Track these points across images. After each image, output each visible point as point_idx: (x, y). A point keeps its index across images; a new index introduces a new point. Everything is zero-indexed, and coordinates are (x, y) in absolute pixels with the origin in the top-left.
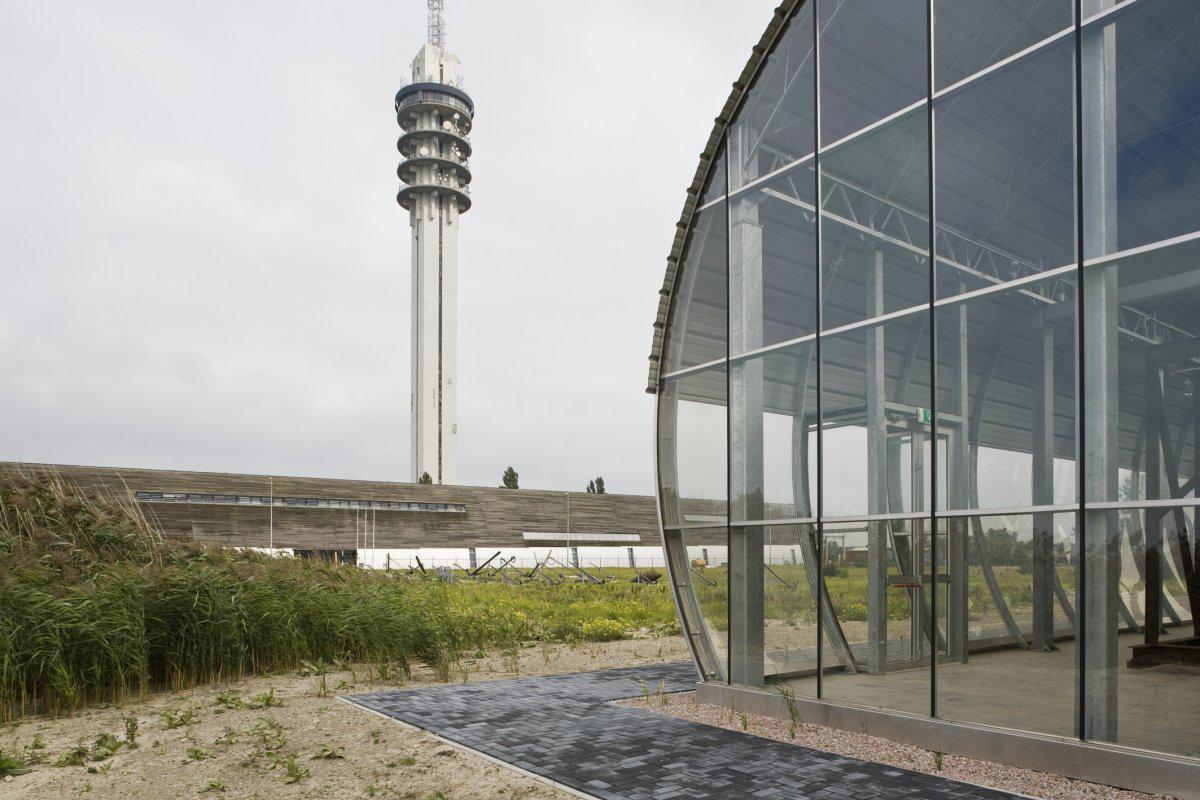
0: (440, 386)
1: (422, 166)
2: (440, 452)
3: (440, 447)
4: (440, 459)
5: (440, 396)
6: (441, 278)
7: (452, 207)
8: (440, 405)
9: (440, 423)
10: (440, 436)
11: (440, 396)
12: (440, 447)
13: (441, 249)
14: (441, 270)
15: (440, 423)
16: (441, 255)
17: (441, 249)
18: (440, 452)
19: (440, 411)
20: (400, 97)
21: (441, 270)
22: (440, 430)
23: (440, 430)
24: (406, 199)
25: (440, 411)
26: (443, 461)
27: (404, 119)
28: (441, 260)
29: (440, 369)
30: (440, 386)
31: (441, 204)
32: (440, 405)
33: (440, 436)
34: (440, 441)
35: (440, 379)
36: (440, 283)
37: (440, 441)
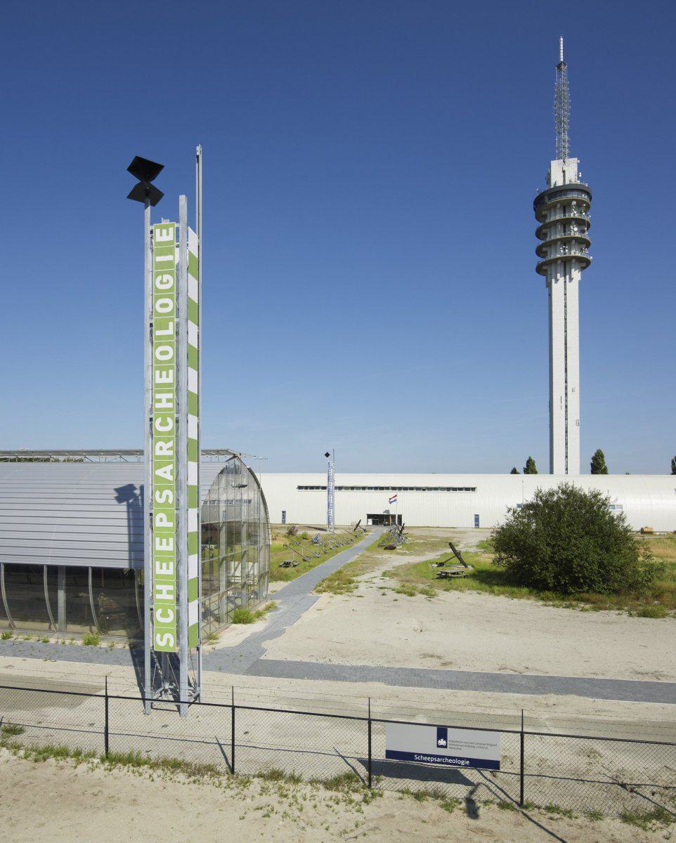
0: (566, 394)
1: (551, 246)
3: (566, 436)
5: (566, 401)
6: (566, 319)
7: (573, 270)
8: (566, 407)
9: (566, 419)
10: (566, 428)
11: (566, 401)
12: (566, 436)
13: (565, 299)
14: (566, 314)
16: (565, 303)
17: (565, 299)
19: (566, 411)
21: (566, 314)
22: (566, 425)
23: (566, 425)
24: (540, 269)
25: (566, 411)
27: (540, 217)
28: (565, 307)
29: (566, 382)
30: (566, 394)
31: (565, 268)
32: (566, 407)
33: (566, 428)
34: (566, 432)
35: (566, 389)
36: (566, 323)
37: (566, 432)
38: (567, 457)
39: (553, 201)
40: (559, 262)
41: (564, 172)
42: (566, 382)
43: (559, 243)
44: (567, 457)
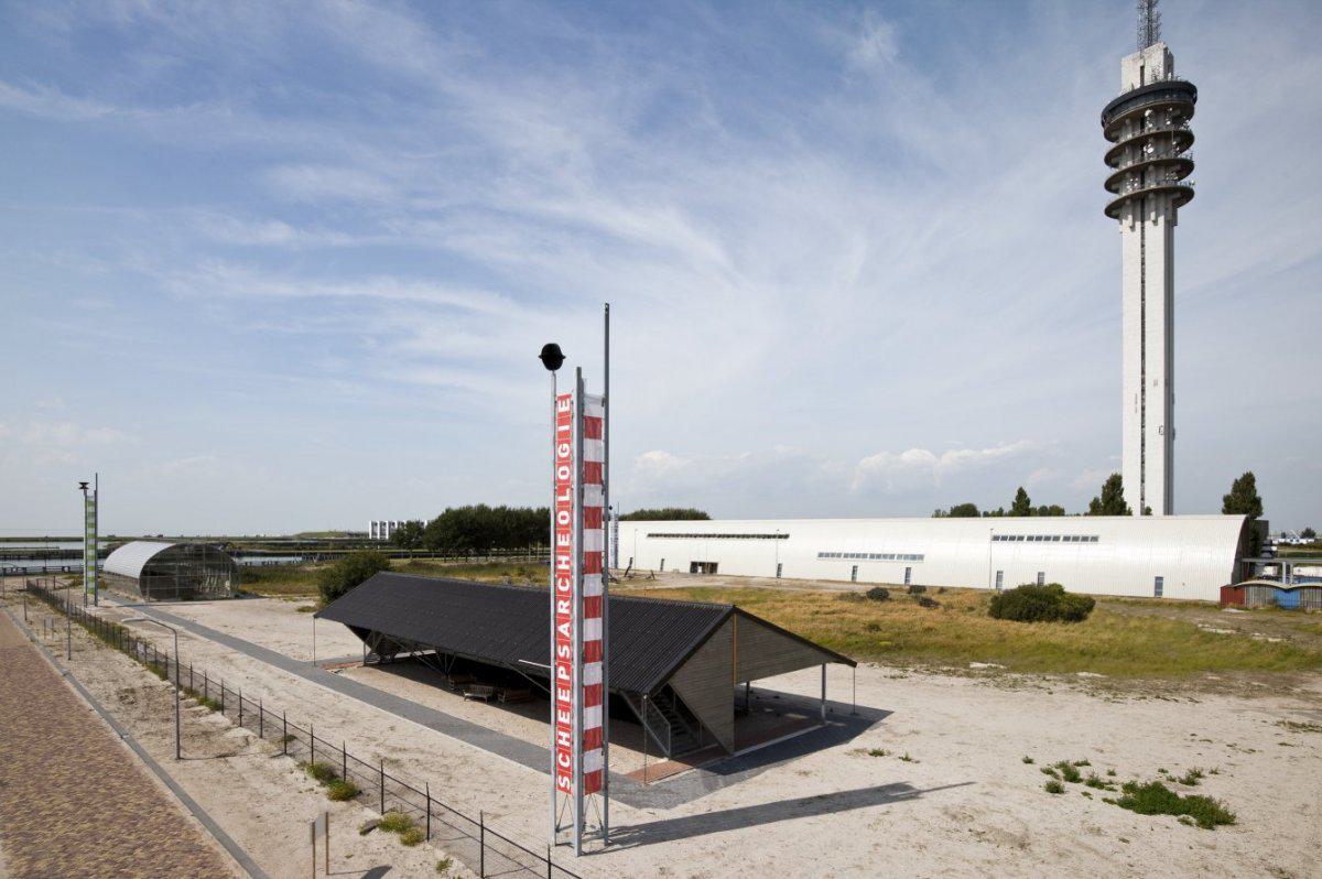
0: (1143, 390)
2: (1143, 456)
3: (1143, 451)
4: (1143, 462)
5: (1143, 399)
6: (1143, 282)
8: (1143, 409)
10: (1143, 439)
11: (1143, 399)
12: (1143, 451)
13: (1143, 253)
14: (1143, 274)
15: (1143, 427)
16: (1143, 259)
17: (1143, 253)
18: (1143, 456)
19: (1143, 415)
20: (1104, 116)
21: (1143, 274)
25: (1143, 415)
26: (1140, 461)
28: (1143, 264)
30: (1143, 390)
32: (1143, 409)
33: (1143, 439)
34: (1143, 445)
35: (1143, 382)
37: (1143, 445)
38: (1143, 481)
39: (1117, 117)
40: (1128, 202)
41: (1142, 68)
42: (1143, 372)
43: (1128, 175)
44: (1143, 481)
